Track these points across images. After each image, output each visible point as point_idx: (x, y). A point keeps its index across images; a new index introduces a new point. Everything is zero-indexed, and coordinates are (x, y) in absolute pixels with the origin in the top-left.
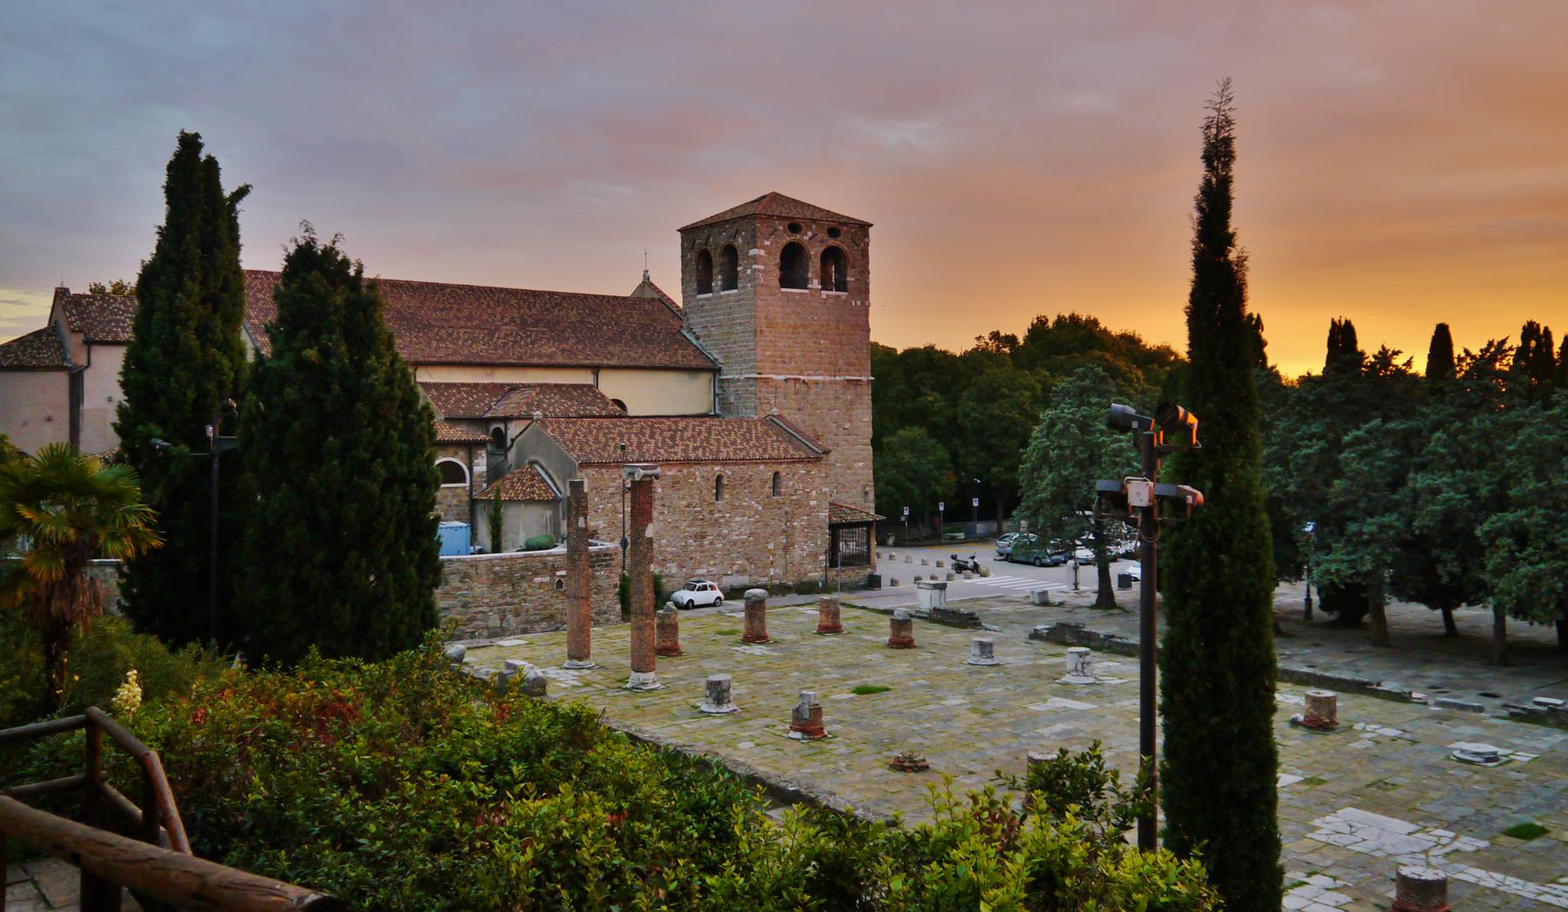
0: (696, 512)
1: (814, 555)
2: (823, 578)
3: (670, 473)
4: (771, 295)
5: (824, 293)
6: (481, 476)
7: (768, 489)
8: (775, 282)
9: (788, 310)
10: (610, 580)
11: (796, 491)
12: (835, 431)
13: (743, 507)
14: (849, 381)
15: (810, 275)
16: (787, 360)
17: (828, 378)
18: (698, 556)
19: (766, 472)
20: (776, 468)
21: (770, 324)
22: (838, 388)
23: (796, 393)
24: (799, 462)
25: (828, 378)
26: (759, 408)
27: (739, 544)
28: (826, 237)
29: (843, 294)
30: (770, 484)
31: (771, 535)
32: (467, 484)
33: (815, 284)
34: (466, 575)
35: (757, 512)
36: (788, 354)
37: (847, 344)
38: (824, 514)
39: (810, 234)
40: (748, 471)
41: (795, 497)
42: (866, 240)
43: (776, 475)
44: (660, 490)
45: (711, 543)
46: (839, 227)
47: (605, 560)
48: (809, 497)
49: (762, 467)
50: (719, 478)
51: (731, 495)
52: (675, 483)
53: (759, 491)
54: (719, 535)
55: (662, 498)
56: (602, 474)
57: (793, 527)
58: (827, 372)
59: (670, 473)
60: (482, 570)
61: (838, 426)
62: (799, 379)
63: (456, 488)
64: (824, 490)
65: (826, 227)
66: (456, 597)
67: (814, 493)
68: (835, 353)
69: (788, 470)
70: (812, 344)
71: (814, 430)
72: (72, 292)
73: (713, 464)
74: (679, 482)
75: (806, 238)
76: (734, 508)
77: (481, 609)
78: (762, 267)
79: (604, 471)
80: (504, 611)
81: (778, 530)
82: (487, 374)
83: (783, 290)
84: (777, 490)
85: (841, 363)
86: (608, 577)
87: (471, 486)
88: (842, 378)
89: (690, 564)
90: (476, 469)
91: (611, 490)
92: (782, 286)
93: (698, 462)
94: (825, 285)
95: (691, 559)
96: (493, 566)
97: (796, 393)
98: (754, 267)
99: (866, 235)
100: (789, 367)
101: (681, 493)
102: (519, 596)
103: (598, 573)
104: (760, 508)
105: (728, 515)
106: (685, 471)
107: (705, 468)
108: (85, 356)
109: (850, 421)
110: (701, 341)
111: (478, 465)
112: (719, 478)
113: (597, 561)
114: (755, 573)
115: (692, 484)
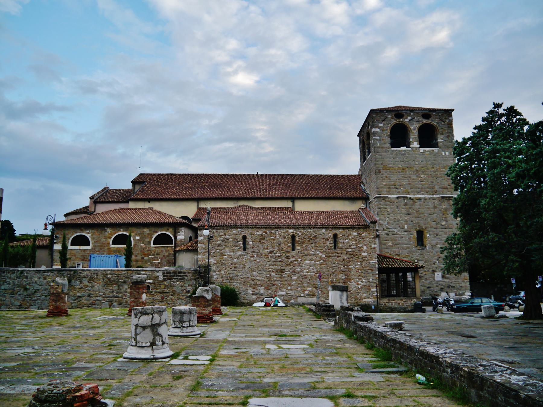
0: (276, 257)
1: (367, 288)
2: (376, 303)
3: (258, 233)
4: (385, 152)
5: (422, 150)
6: (181, 241)
7: (329, 244)
8: (389, 145)
9: (397, 159)
10: (183, 288)
11: (351, 246)
12: (435, 226)
13: (310, 255)
14: (443, 197)
15: (411, 140)
16: (398, 187)
17: (427, 196)
18: (279, 283)
19: (330, 234)
20: (335, 231)
21: (385, 168)
22: (436, 201)
23: (406, 205)
24: (352, 228)
25: (427, 196)
26: (380, 213)
27: (309, 278)
28: (421, 119)
29: (436, 149)
30: (331, 241)
31: (333, 273)
32: (173, 245)
33: (416, 144)
34: (91, 279)
35: (321, 258)
36: (399, 184)
37: (441, 177)
38: (374, 261)
39: (409, 118)
40: (313, 233)
41: (350, 250)
42: (450, 118)
43: (335, 236)
44: (251, 243)
45: (288, 276)
46: (431, 113)
47: (180, 276)
48: (361, 250)
49: (324, 231)
50: (293, 237)
51: (302, 247)
52: (261, 239)
53: (322, 245)
54: (294, 271)
55: (253, 248)
56: (213, 233)
57: (350, 269)
58: (427, 192)
59: (258, 233)
60: (100, 276)
61: (437, 224)
62: (407, 197)
63: (167, 247)
64: (373, 246)
65: (421, 114)
66: (85, 291)
67: (365, 248)
68: (432, 182)
69: (343, 233)
70: (415, 178)
71: (419, 226)
72: (110, 188)
73: (288, 228)
74: (264, 239)
75: (407, 120)
76: (303, 255)
77: (98, 298)
78: (378, 138)
79: (214, 231)
80: (112, 300)
81: (338, 271)
82: (234, 203)
83: (393, 149)
84: (338, 245)
85: (437, 187)
86: (181, 286)
87: (175, 246)
88: (438, 196)
89: (274, 288)
90: (179, 238)
91: (219, 242)
92: (392, 147)
93: (277, 227)
94: (422, 144)
95: (274, 285)
96: (107, 274)
97: (406, 205)
98: (374, 138)
99: (451, 116)
100: (400, 190)
101: (266, 245)
102: (121, 293)
103: (174, 283)
104: (324, 256)
105: (300, 259)
106: (268, 232)
107: (282, 231)
108: (94, 208)
109: (446, 221)
110: (365, 187)
111: (180, 236)
112: (293, 237)
113: (174, 276)
114: (322, 297)
115: (274, 240)
